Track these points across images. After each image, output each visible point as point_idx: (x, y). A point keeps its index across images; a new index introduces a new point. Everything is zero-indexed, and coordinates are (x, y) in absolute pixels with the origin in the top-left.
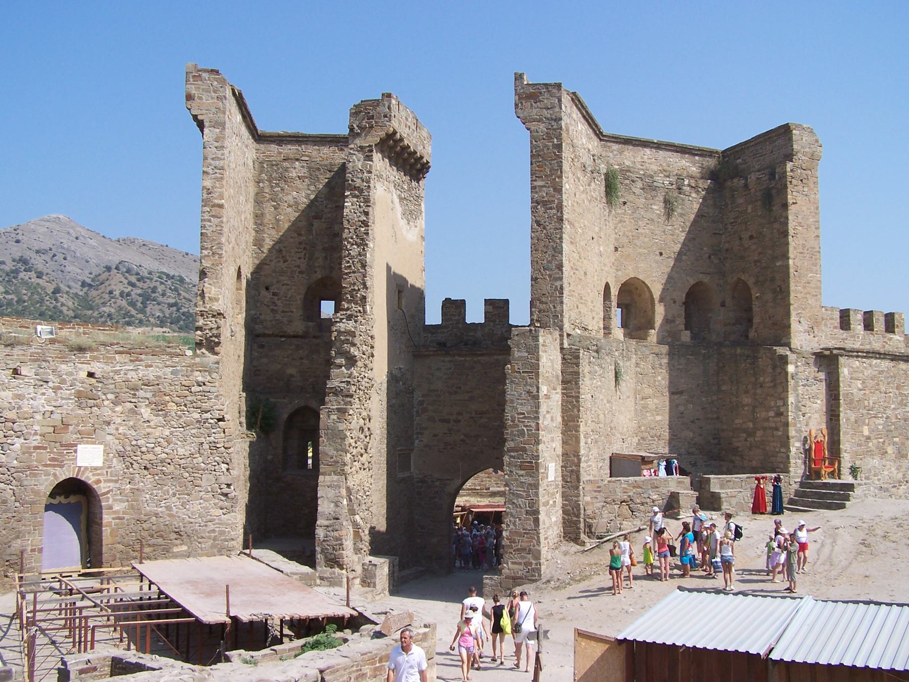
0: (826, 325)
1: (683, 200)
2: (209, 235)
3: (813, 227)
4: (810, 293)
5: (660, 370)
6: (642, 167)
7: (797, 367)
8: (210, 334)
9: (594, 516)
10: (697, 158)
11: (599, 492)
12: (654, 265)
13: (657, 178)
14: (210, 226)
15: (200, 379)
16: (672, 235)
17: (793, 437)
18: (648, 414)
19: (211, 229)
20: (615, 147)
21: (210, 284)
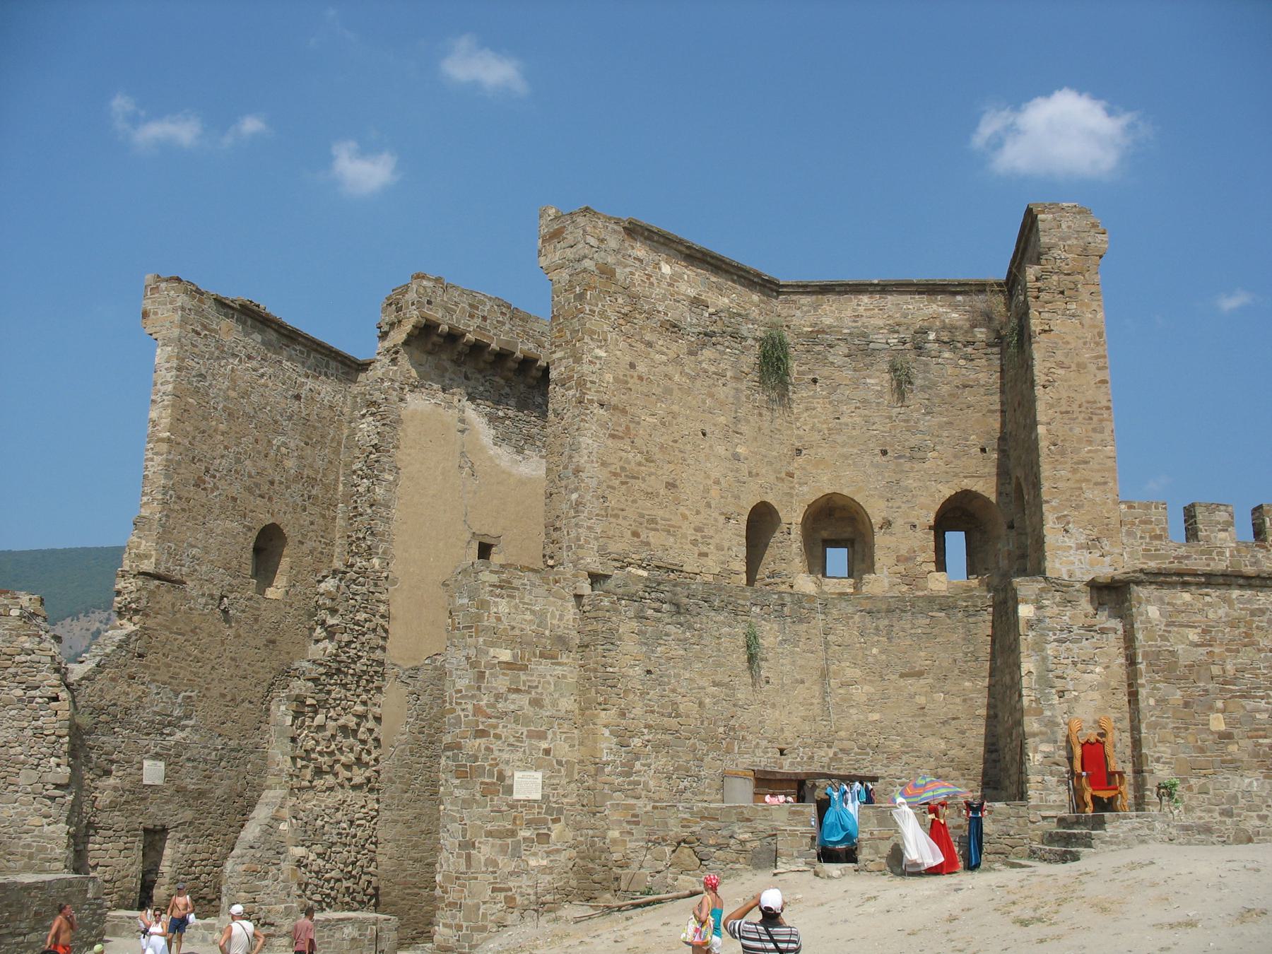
0: (1130, 534)
1: (926, 365)
2: (150, 477)
3: (1092, 367)
4: (1088, 481)
5: (876, 638)
6: (854, 324)
7: (1039, 608)
8: (129, 600)
9: (626, 863)
10: (959, 298)
11: (637, 823)
12: (871, 471)
13: (876, 336)
14: (153, 466)
15: (27, 645)
16: (907, 421)
17: (1034, 735)
18: (852, 711)
19: (152, 470)
20: (805, 300)
21: (140, 537)
